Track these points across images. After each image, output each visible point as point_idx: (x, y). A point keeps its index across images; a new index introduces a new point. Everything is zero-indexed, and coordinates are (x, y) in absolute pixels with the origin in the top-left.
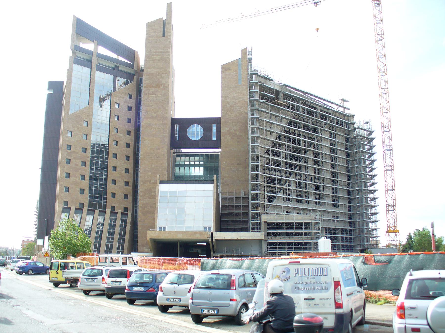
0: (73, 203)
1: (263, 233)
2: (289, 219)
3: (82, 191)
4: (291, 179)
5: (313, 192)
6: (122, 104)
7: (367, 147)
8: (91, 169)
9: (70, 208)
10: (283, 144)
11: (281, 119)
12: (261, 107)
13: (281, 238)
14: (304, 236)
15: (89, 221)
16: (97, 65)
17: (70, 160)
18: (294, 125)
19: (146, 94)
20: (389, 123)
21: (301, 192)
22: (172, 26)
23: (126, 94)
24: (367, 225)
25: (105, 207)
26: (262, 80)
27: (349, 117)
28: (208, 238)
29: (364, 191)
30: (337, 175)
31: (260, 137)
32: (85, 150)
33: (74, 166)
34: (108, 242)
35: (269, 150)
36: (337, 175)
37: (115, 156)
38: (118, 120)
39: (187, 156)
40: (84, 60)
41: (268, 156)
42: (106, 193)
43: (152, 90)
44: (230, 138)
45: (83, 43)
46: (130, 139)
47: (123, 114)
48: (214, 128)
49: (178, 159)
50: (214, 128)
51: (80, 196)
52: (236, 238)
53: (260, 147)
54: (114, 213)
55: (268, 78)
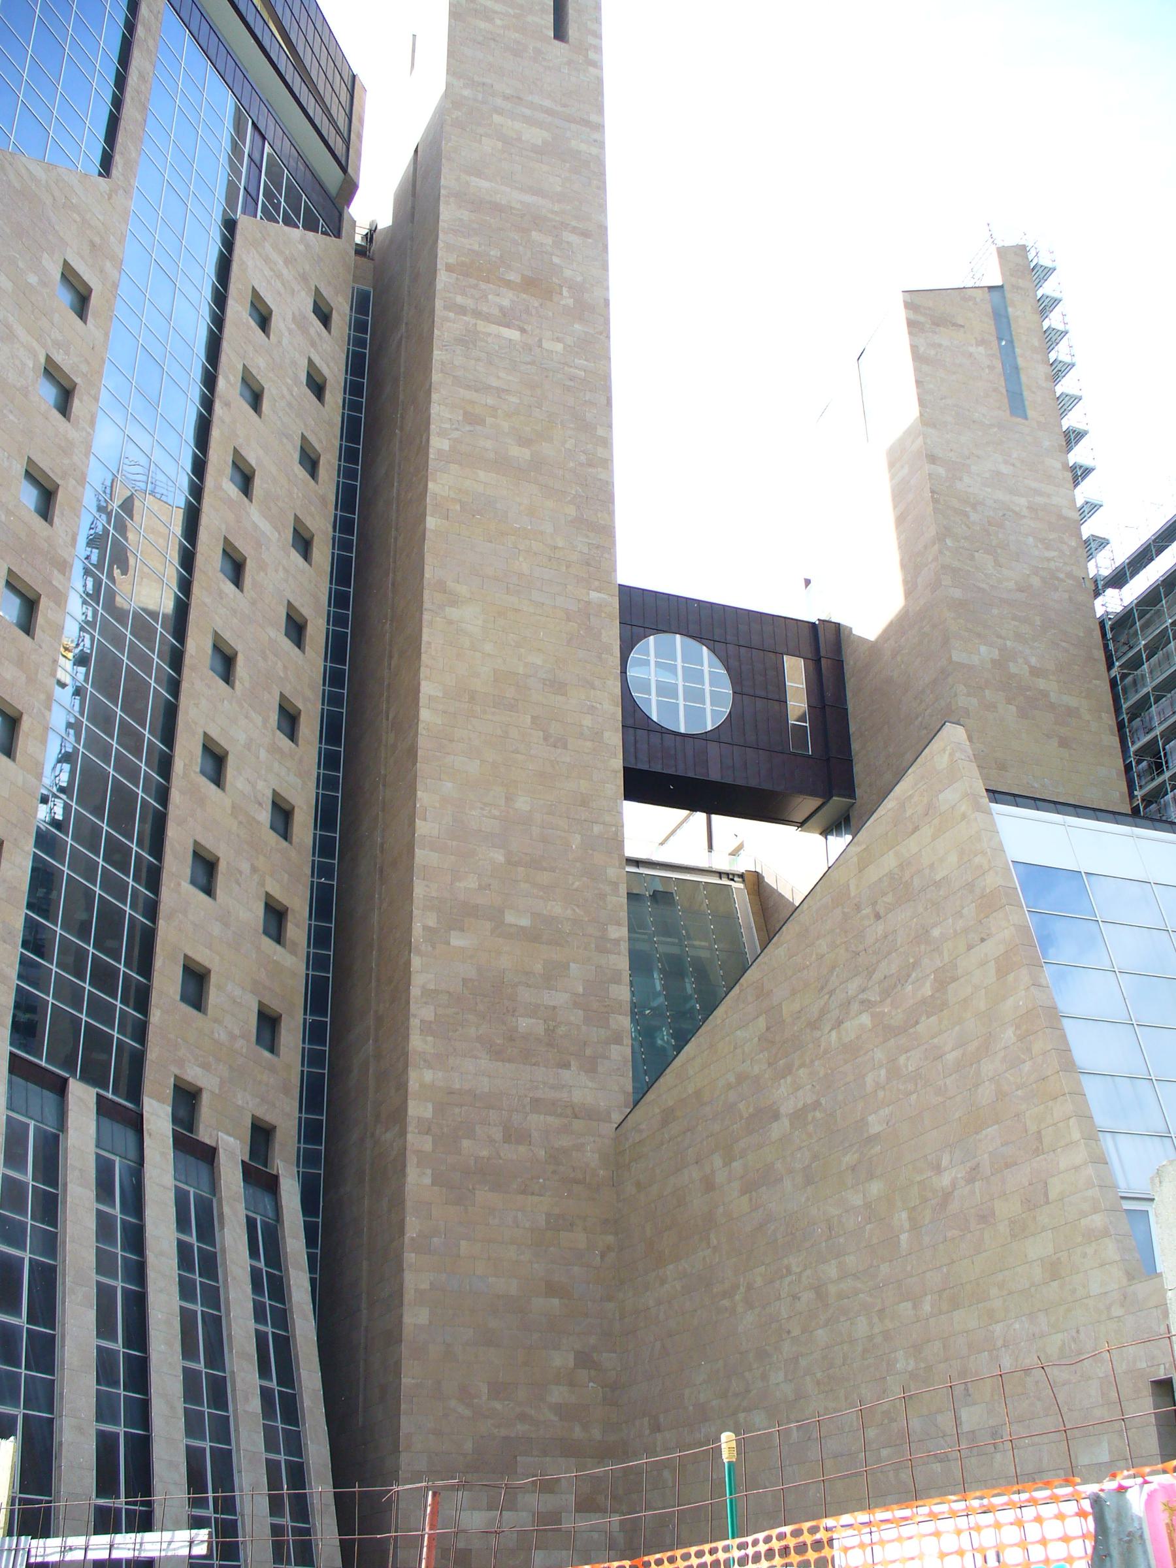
6: (282, 326)
19: (462, 310)
23: (304, 278)
43: (506, 299)
44: (1013, 708)
47: (285, 392)
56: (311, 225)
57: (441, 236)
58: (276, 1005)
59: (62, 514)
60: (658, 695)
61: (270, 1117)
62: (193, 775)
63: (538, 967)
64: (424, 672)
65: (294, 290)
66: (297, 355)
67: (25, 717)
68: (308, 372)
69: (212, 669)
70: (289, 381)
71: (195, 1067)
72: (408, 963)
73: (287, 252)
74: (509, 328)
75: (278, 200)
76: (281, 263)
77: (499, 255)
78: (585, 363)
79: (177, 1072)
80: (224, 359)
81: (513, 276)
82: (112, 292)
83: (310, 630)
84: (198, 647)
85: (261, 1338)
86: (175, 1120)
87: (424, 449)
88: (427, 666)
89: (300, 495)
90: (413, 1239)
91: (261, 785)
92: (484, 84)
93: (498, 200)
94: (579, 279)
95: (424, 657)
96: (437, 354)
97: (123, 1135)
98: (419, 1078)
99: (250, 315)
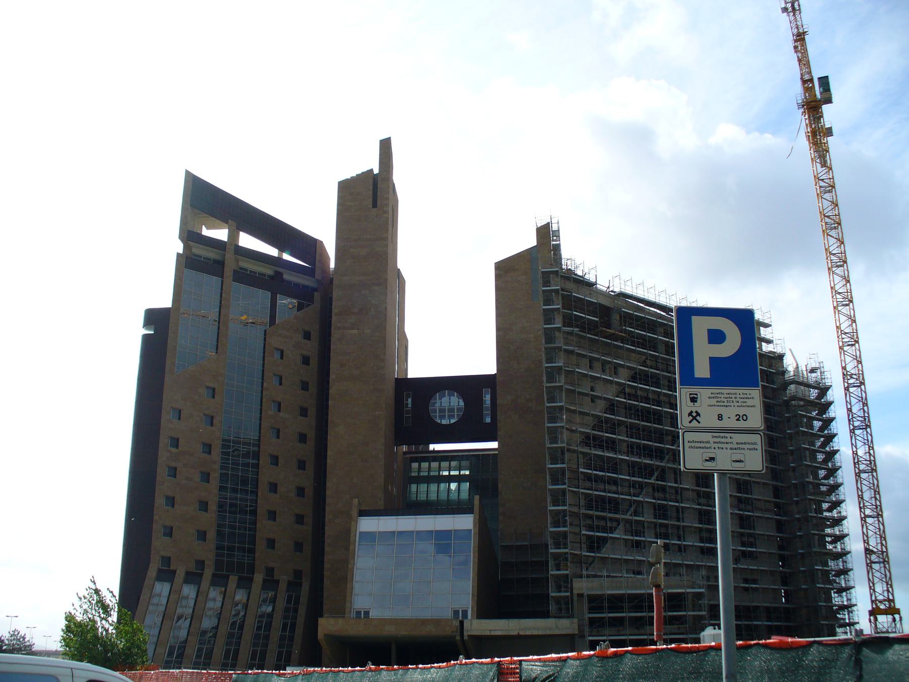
1: (575, 620)
2: (636, 588)
3: (202, 535)
4: (642, 499)
5: (695, 527)
7: (817, 424)
8: (221, 488)
9: (174, 572)
10: (620, 423)
11: (616, 368)
12: (567, 344)
13: (619, 631)
14: (669, 625)
15: (214, 600)
16: (234, 271)
17: (176, 469)
18: (645, 380)
20: (860, 365)
21: (666, 526)
22: (391, 187)
24: (829, 599)
25: (252, 569)
26: (570, 285)
27: (773, 361)
28: (454, 634)
29: (815, 521)
30: (751, 487)
31: (567, 409)
32: (208, 448)
34: (255, 645)
35: (587, 436)
36: (749, 487)
37: (275, 460)
38: (281, 384)
39: (435, 459)
40: (208, 261)
41: (586, 450)
42: (253, 541)
45: (208, 228)
46: (307, 425)
48: (487, 398)
49: (415, 465)
50: (487, 398)
52: (515, 633)
53: (567, 429)
54: (270, 583)
55: (583, 281)
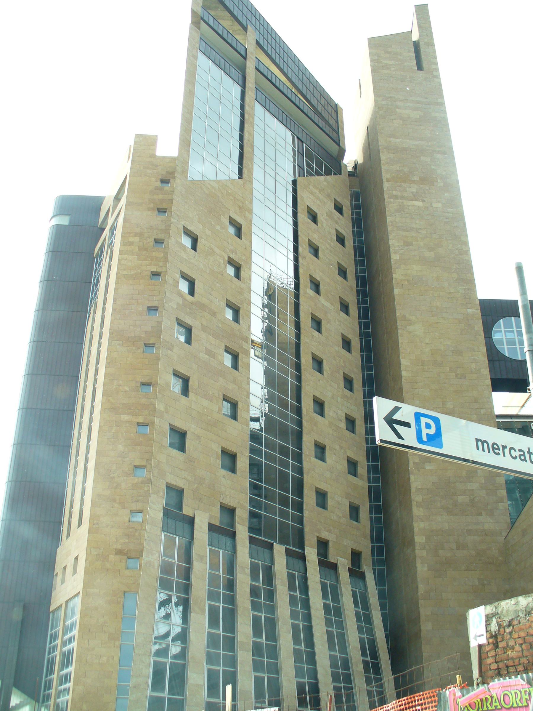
0: (200, 500)
6: (322, 219)
9: (191, 521)
19: (396, 197)
23: (328, 196)
33: (202, 355)
51: (224, 477)
56: (328, 173)
57: (383, 167)
58: (356, 502)
59: (243, 319)
60: (507, 345)
61: (358, 548)
62: (310, 413)
63: (464, 474)
64: (401, 356)
65: (325, 202)
66: (331, 229)
67: (239, 403)
68: (336, 234)
69: (313, 369)
70: (329, 241)
71: (325, 532)
72: (409, 479)
73: (320, 187)
74: (417, 201)
75: (312, 166)
76: (318, 192)
77: (408, 170)
78: (452, 210)
79: (317, 535)
80: (300, 239)
81: (415, 178)
82: (250, 224)
83: (353, 343)
84: (306, 361)
85: (362, 640)
86: (319, 554)
87: (389, 259)
88: (402, 353)
89: (341, 288)
90: (422, 594)
91: (340, 412)
92: (391, 97)
93: (404, 146)
94: (444, 173)
95: (400, 349)
96: (389, 219)
97: (298, 563)
98: (418, 526)
99: (308, 218)
